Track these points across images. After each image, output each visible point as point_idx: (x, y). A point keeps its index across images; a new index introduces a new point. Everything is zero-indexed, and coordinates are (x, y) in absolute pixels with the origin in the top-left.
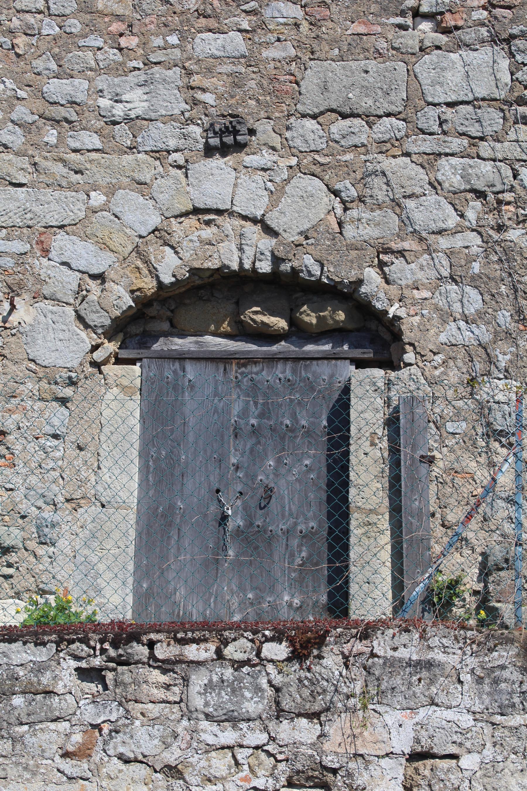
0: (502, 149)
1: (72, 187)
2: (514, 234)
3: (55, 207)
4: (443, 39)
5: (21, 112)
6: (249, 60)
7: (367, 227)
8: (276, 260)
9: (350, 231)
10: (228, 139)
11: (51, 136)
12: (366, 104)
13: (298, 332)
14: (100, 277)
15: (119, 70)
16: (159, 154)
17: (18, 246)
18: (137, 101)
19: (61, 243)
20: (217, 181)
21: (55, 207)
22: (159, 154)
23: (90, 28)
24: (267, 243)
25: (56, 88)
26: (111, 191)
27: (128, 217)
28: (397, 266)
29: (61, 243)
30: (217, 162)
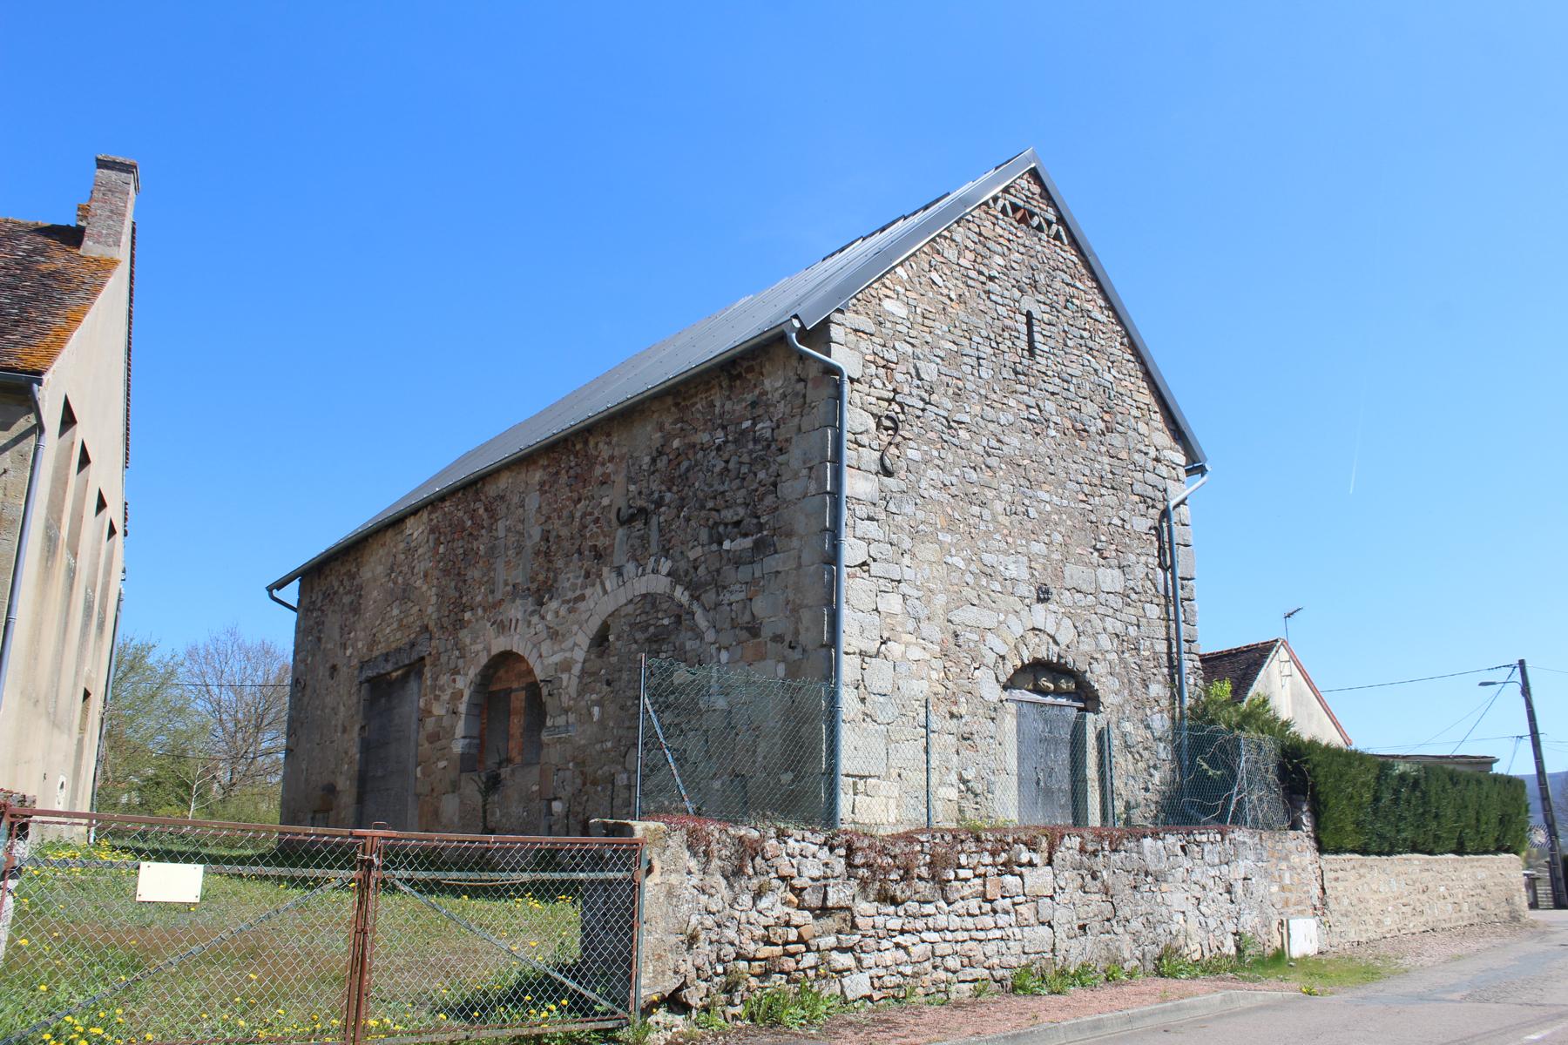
0: (1124, 617)
1: (992, 609)
2: (1126, 655)
3: (988, 619)
4: (1102, 561)
5: (973, 567)
6: (1046, 557)
7: (1087, 646)
8: (1060, 657)
9: (1081, 647)
10: (1043, 596)
11: (984, 582)
12: (1084, 588)
13: (1058, 693)
14: (1003, 657)
15: (1006, 553)
16: (1022, 598)
17: (976, 637)
18: (1013, 572)
19: (989, 636)
20: (1040, 615)
21: (988, 619)
22: (1022, 598)
23: (997, 531)
24: (1056, 649)
25: (985, 556)
26: (1007, 613)
27: (1014, 628)
28: (1095, 665)
29: (989, 636)
30: (1040, 606)
